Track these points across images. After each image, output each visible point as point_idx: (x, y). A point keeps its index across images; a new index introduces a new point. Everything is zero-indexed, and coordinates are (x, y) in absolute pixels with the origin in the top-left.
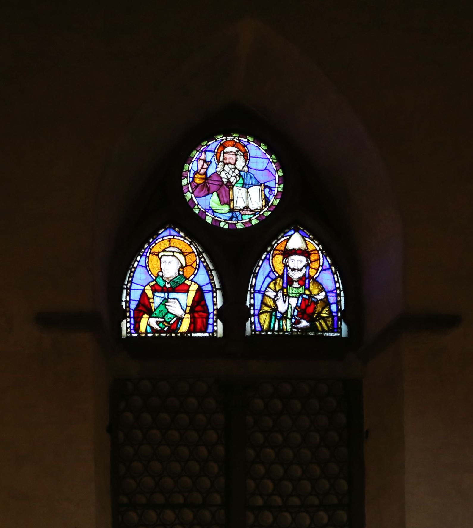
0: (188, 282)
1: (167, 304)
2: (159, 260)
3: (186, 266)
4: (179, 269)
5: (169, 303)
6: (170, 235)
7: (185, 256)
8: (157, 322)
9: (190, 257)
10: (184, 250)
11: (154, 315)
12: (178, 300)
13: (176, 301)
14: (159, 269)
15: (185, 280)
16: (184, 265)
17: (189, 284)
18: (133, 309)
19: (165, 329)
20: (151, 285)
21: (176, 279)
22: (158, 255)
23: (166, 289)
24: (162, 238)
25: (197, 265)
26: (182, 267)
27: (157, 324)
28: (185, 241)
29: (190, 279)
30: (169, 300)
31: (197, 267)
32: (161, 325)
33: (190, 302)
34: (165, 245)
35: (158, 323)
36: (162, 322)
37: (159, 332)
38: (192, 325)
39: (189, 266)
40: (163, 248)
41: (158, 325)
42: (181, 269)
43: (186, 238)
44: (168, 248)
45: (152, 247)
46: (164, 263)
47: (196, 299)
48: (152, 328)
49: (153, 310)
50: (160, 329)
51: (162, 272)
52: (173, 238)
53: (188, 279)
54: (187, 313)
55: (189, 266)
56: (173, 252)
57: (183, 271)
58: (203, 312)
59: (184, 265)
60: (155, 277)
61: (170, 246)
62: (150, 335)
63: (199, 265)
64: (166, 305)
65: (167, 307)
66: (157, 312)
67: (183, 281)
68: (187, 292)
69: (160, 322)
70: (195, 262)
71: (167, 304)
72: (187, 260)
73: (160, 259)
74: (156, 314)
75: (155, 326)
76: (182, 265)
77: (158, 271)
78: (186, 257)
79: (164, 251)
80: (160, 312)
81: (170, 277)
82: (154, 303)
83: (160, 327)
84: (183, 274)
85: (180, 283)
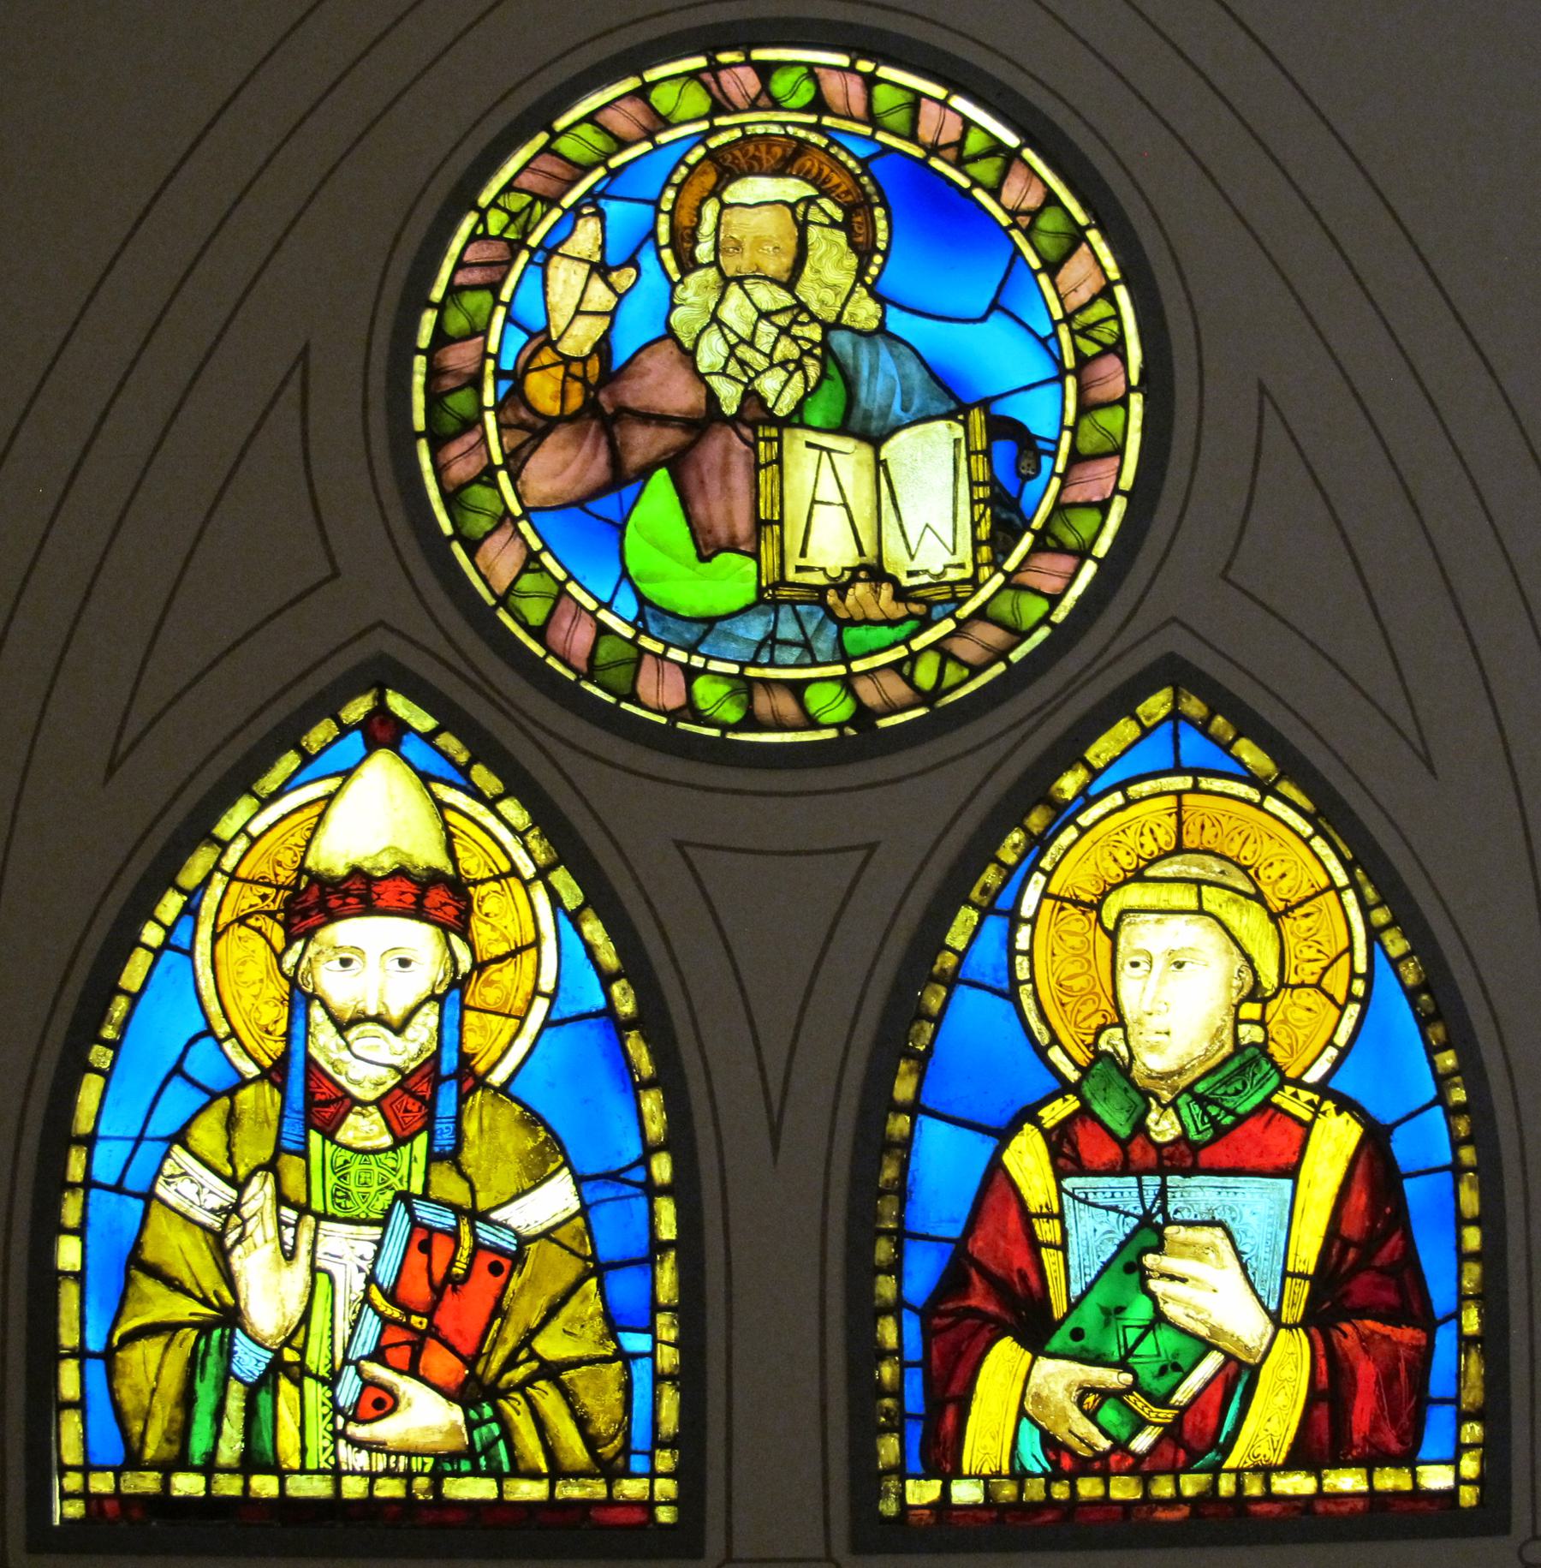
0: (1295, 1104)
1: (1150, 1260)
2: (1104, 943)
3: (1283, 984)
4: (1237, 1007)
5: (1172, 1254)
6: (1178, 770)
7: (1274, 917)
8: (1085, 1391)
9: (1308, 922)
10: (1270, 871)
11: (1059, 1340)
12: (1229, 1235)
13: (1219, 1232)
14: (1106, 1005)
15: (1279, 1087)
16: (1269, 979)
17: (1306, 1116)
18: (919, 1306)
19: (1142, 1443)
20: (1048, 1124)
21: (1211, 1080)
22: (1097, 906)
23: (1153, 1154)
24: (1122, 786)
25: (1353, 975)
26: (1255, 994)
27: (1080, 1403)
28: (1272, 804)
29: (1312, 1077)
30: (1169, 1230)
31: (1359, 988)
32: (1109, 1415)
33: (1307, 1254)
34: (1147, 839)
35: (1091, 1399)
36: (1117, 1395)
37: (1098, 1465)
38: (1322, 1411)
39: (1302, 985)
40: (1128, 862)
41: (1091, 1416)
42: (1251, 1010)
43: (1285, 788)
44: (1167, 855)
45: (1054, 851)
46: (1135, 965)
47: (1353, 1228)
48: (1049, 1442)
49: (1059, 1307)
50: (1104, 1444)
51: (1121, 1024)
52: (1196, 789)
53: (1298, 1083)
54: (1289, 1327)
55: (1302, 985)
56: (1199, 882)
57: (1262, 1023)
58: (1393, 1317)
59: (1269, 979)
60: (1077, 1067)
61: (1179, 849)
62: (1035, 1490)
63: (1369, 978)
64: (1144, 1275)
65: (1153, 1285)
66: (1088, 1316)
67: (1257, 1098)
68: (1291, 1172)
69: (1105, 1394)
70: (1346, 958)
71: (1150, 1260)
72: (1291, 942)
73: (1113, 935)
74: (1077, 1334)
75: (1080, 1430)
76: (1257, 983)
77: (1097, 1020)
78: (1287, 924)
79: (1138, 876)
80: (1107, 1323)
81: (1180, 1072)
82: (1063, 1247)
83: (1105, 1433)
84: (1263, 1048)
85: (1241, 1110)
